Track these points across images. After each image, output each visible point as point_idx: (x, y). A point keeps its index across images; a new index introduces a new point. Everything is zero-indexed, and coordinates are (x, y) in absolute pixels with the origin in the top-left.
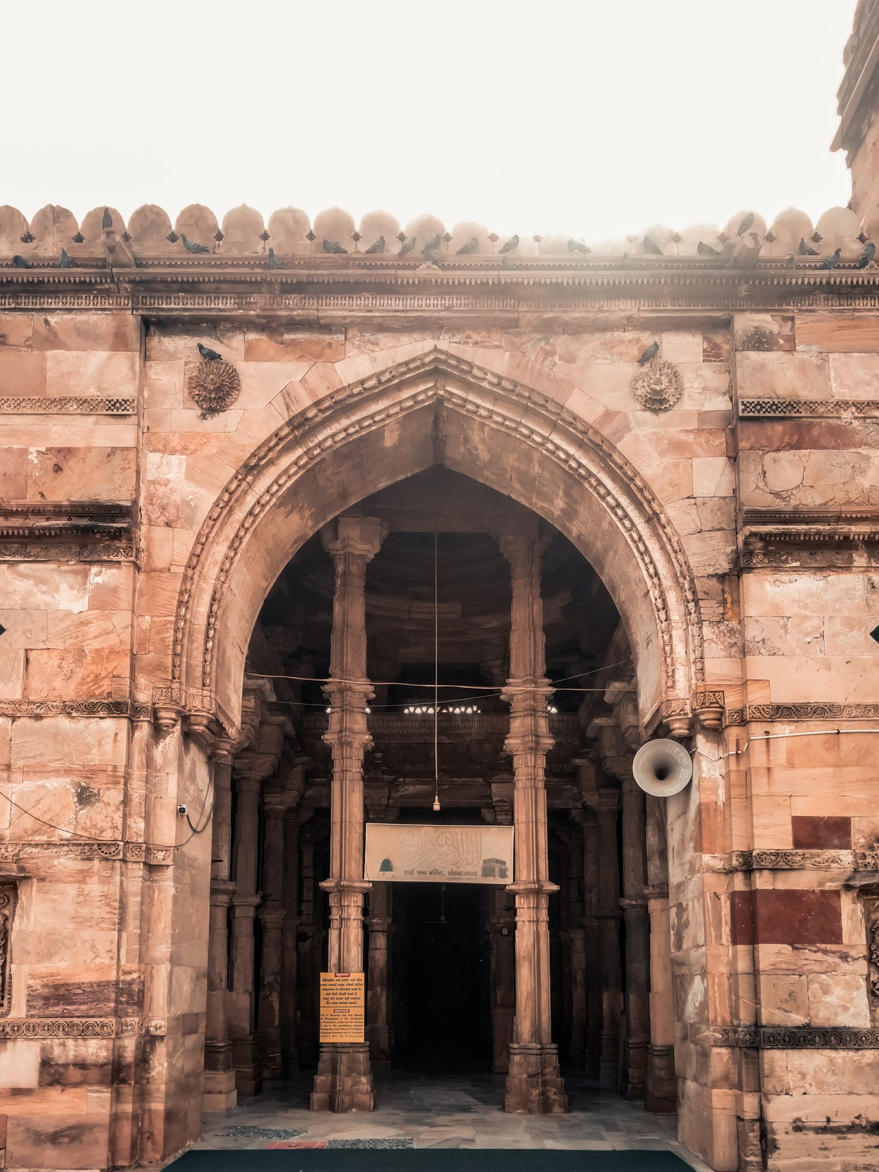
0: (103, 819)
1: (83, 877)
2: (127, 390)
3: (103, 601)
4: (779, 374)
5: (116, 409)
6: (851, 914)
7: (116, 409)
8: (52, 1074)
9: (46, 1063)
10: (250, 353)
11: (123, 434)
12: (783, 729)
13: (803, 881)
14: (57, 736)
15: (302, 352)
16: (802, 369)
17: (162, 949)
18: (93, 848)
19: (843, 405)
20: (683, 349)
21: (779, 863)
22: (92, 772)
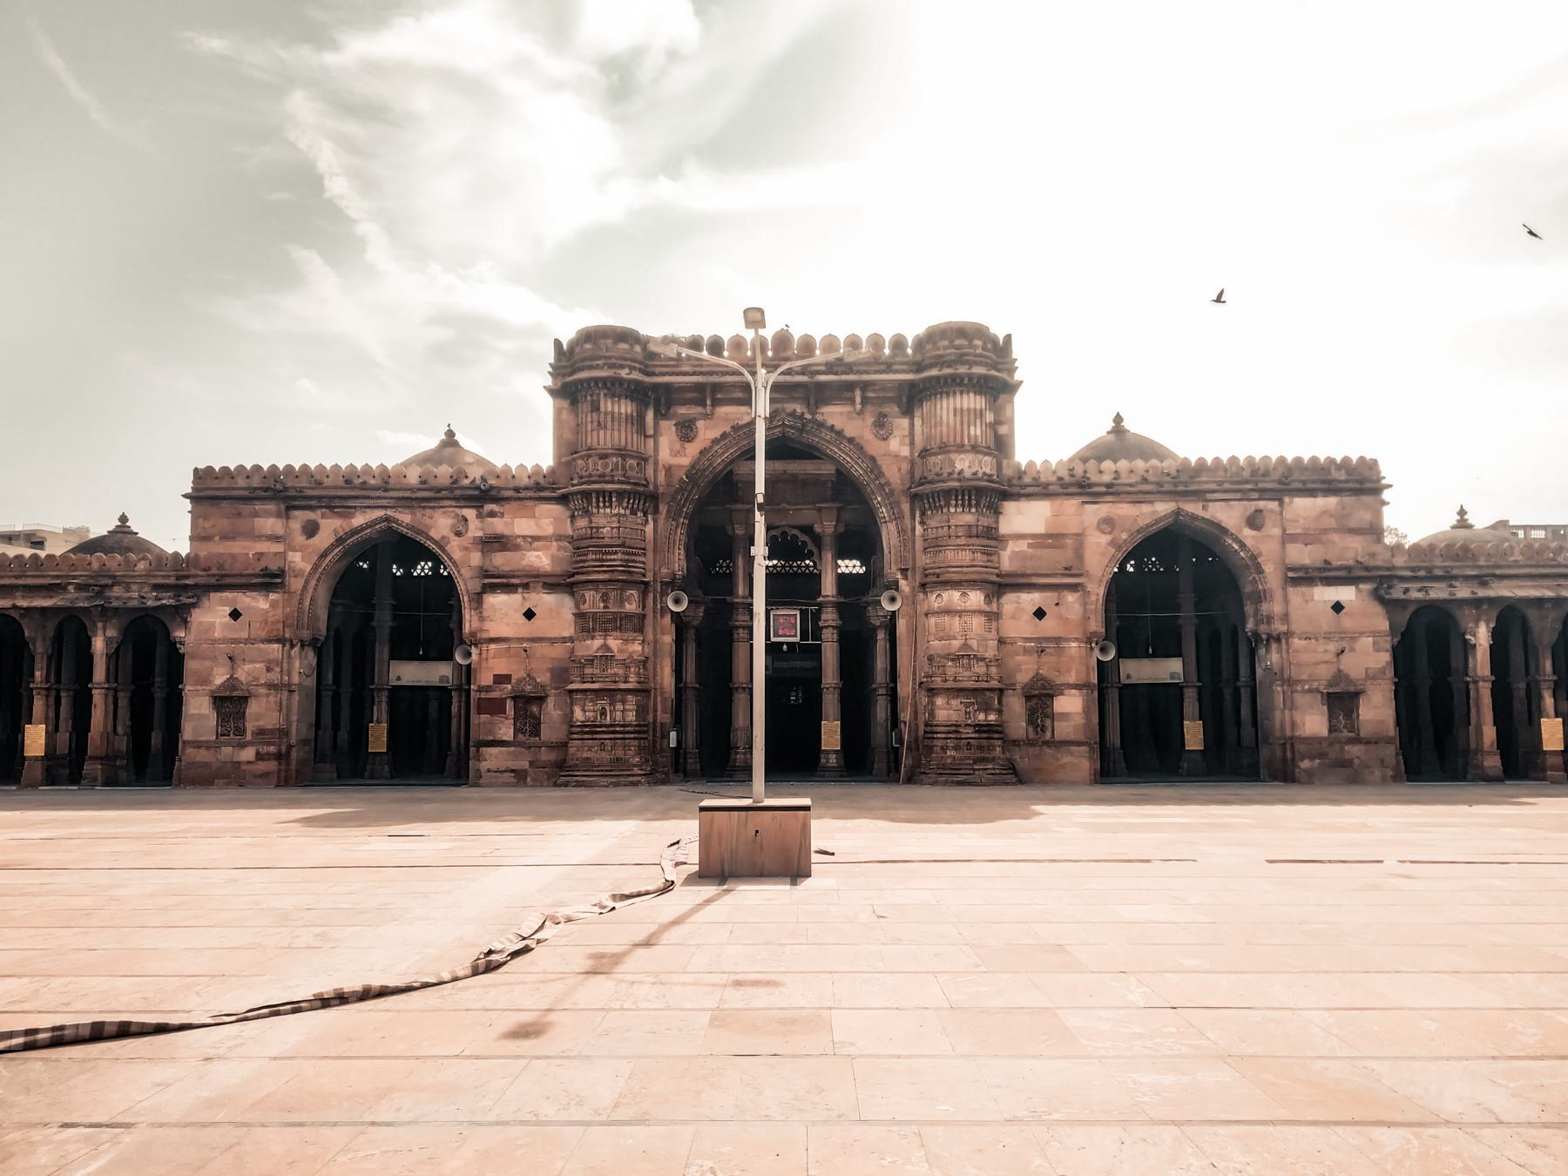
0: (275, 676)
1: (268, 695)
2: (281, 532)
3: (274, 605)
4: (498, 525)
5: (276, 538)
6: (509, 704)
7: (276, 538)
8: (260, 757)
9: (258, 753)
10: (323, 516)
11: (279, 548)
12: (493, 646)
14: (259, 650)
16: (506, 524)
17: (295, 718)
18: (271, 686)
20: (470, 513)
21: (488, 689)
22: (270, 662)
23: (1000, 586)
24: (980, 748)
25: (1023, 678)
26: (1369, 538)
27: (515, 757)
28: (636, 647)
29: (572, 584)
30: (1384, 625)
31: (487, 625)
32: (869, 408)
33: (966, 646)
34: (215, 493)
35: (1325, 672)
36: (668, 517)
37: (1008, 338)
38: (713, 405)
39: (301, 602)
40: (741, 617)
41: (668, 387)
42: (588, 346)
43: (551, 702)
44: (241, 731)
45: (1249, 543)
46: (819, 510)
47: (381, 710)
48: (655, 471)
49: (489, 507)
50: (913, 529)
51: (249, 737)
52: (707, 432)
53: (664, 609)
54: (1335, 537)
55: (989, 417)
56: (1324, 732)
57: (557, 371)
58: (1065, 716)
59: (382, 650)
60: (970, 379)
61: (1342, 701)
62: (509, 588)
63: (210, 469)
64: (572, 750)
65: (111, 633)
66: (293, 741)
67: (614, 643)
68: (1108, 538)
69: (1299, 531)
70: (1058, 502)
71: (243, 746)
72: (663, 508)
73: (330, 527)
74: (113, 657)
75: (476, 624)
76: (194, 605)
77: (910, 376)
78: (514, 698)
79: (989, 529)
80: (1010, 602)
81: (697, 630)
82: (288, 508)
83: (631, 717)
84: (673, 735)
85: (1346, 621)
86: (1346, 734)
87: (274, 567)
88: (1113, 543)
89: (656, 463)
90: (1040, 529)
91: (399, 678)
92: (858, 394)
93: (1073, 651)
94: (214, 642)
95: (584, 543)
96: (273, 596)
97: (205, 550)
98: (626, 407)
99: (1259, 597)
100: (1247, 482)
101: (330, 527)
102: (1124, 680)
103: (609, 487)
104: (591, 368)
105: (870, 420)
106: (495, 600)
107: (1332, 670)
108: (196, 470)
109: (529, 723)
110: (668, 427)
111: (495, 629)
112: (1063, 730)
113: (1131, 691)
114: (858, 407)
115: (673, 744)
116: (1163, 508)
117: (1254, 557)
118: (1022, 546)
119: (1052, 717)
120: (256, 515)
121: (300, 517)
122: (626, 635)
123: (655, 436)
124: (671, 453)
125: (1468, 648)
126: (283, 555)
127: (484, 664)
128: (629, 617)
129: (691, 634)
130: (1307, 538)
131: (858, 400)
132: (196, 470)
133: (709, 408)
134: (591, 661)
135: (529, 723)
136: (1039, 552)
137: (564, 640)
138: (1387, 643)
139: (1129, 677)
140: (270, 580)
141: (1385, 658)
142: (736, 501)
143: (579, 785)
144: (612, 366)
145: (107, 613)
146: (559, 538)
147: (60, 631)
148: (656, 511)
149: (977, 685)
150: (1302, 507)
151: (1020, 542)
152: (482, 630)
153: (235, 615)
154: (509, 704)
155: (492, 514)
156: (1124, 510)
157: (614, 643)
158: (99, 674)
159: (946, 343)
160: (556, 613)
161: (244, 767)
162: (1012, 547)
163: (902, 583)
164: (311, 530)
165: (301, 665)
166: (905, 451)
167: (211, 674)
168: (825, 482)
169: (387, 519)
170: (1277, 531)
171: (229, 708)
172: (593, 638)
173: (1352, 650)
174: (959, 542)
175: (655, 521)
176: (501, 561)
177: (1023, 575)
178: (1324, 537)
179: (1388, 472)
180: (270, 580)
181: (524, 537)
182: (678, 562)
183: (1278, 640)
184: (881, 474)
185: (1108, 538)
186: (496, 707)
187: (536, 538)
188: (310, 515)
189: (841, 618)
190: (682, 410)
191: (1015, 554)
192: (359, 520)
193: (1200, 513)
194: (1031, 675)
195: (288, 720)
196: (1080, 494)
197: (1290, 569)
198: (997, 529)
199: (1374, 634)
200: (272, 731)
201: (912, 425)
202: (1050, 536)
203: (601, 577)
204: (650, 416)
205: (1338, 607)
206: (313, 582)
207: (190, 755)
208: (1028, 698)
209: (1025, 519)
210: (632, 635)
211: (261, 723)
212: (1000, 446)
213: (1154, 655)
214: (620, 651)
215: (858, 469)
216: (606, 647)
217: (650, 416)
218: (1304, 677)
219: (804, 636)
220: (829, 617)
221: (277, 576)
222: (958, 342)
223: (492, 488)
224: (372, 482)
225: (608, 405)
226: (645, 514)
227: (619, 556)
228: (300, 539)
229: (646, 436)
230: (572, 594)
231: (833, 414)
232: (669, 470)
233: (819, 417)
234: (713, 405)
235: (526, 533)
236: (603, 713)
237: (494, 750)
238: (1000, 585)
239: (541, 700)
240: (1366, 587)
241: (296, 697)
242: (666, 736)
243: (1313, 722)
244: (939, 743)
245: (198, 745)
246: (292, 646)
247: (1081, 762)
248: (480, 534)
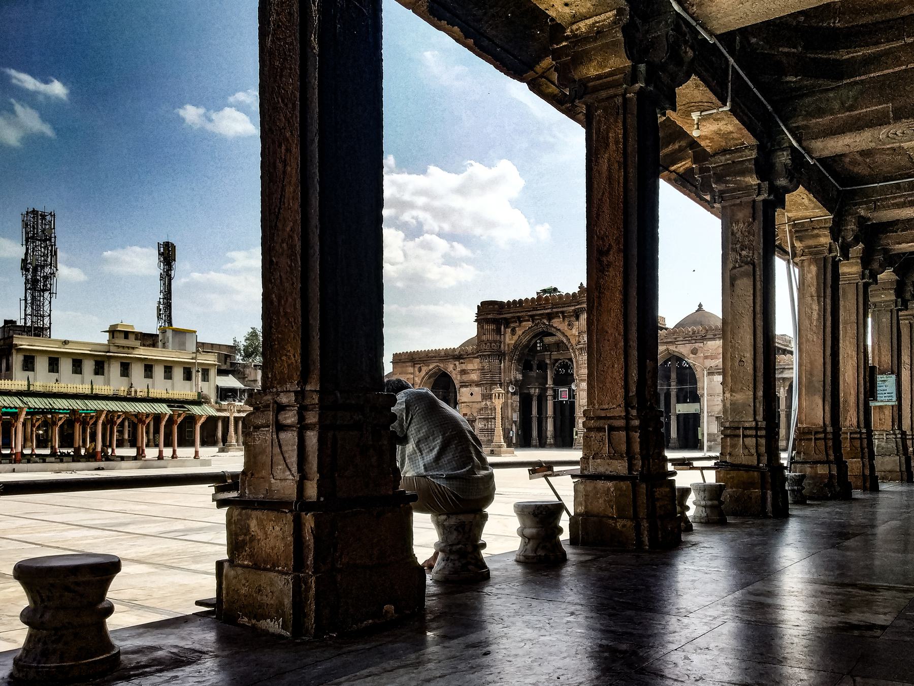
4: (464, 367)
20: (457, 363)
38: (520, 322)
41: (505, 319)
52: (519, 332)
62: (466, 386)
73: (425, 369)
98: (492, 327)
106: (463, 390)
110: (509, 330)
134: (481, 409)
148: (505, 359)
164: (420, 370)
192: (431, 367)
219: (570, 398)
231: (556, 322)
232: (508, 345)
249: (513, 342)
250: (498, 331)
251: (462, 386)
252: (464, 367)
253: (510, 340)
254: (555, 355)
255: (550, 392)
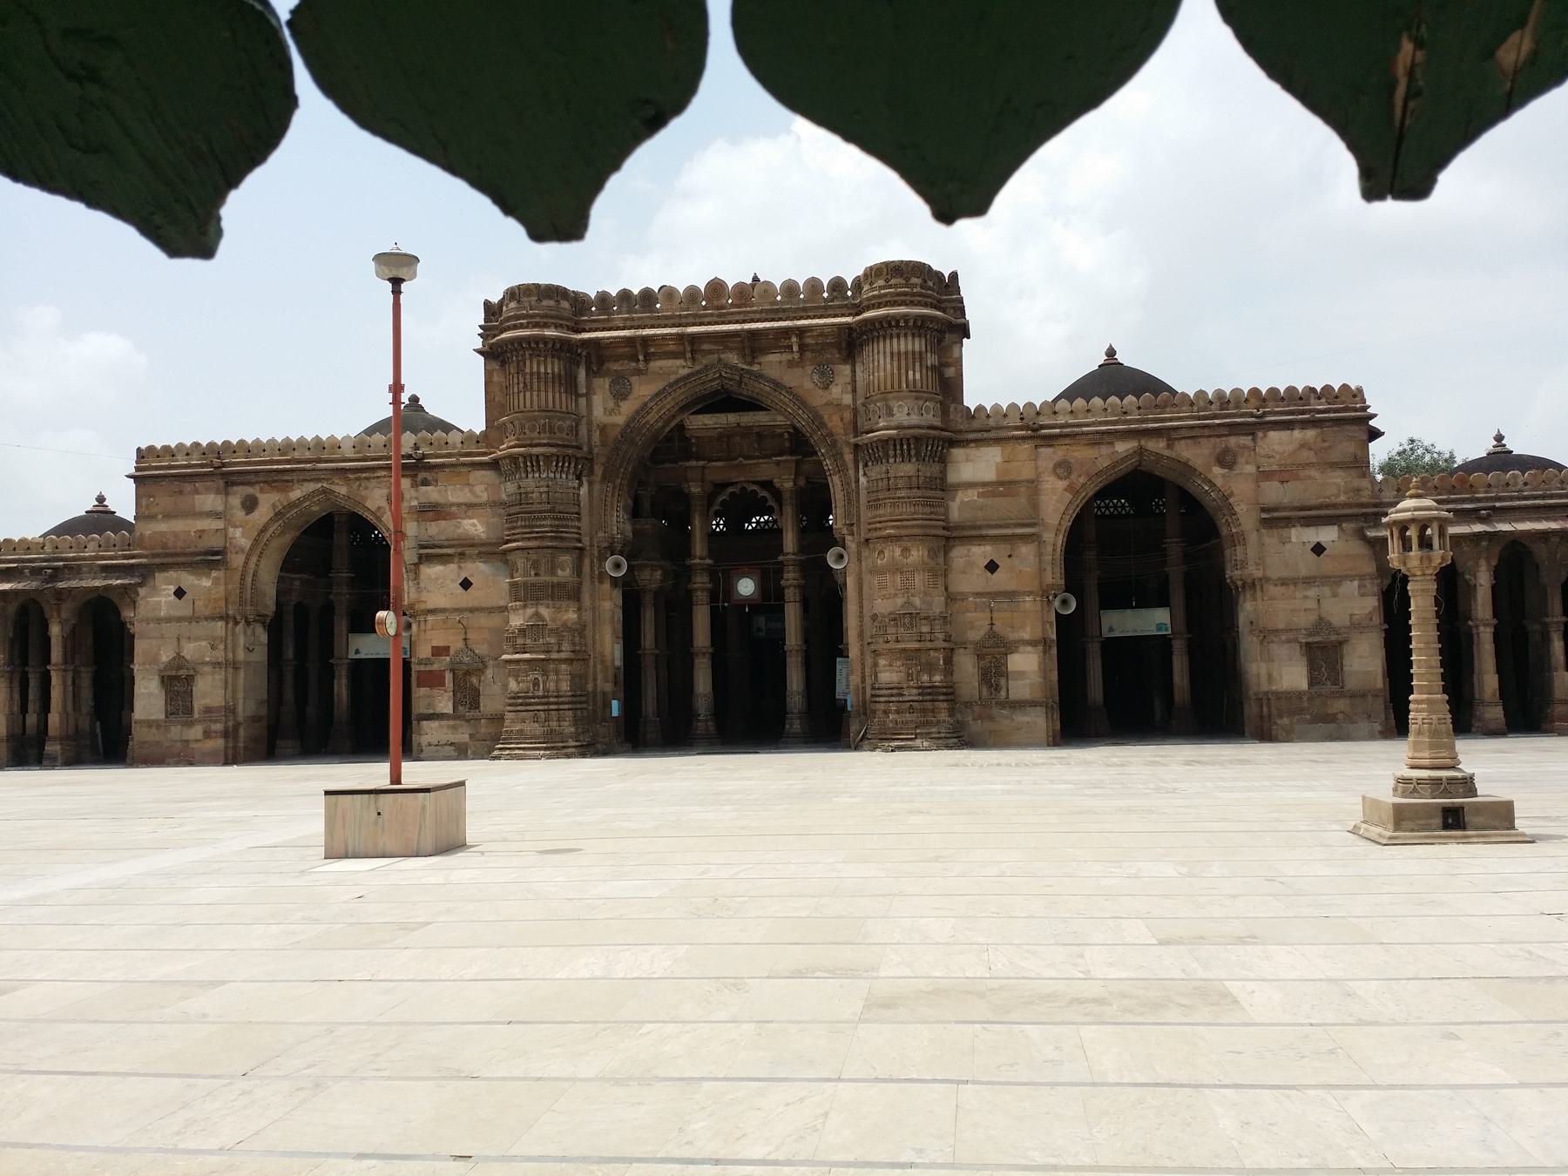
0: (219, 655)
2: (220, 508)
3: (216, 581)
4: (432, 494)
8: (207, 734)
10: (262, 491)
11: (220, 524)
13: (435, 667)
15: (279, 490)
17: (241, 695)
18: (216, 664)
19: (452, 505)
20: (406, 483)
21: (427, 662)
22: (214, 639)
23: (947, 537)
24: (924, 711)
25: (975, 635)
26: (1353, 472)
27: (454, 727)
28: (571, 616)
29: (505, 552)
30: (1371, 568)
31: (425, 596)
32: (809, 355)
33: (908, 603)
34: (158, 473)
35: (1305, 620)
36: (604, 478)
37: (954, 276)
38: (646, 361)
39: (243, 578)
40: (698, 579)
42: (513, 305)
43: (489, 673)
44: (189, 710)
45: (1219, 482)
46: (778, 463)
47: (341, 688)
48: (589, 431)
49: (422, 475)
50: (857, 481)
51: (196, 715)
52: (643, 390)
53: (603, 575)
54: (1313, 473)
55: (931, 360)
56: (1303, 684)
57: (487, 332)
58: (1021, 674)
59: (341, 624)
60: (906, 322)
61: (1323, 654)
62: (444, 559)
63: (151, 449)
64: (507, 723)
65: (64, 615)
66: (241, 719)
67: (545, 612)
68: (1065, 483)
69: (1275, 467)
70: (1009, 447)
71: (190, 724)
72: (599, 470)
73: (268, 502)
74: (71, 640)
75: (413, 596)
76: (141, 585)
77: (849, 319)
78: (453, 671)
79: (932, 479)
80: (959, 554)
81: (657, 594)
82: (227, 484)
83: (565, 686)
84: (615, 704)
85: (1326, 564)
86: (1329, 687)
87: (216, 543)
88: (1069, 489)
89: (590, 423)
90: (989, 475)
91: (357, 652)
92: (794, 339)
93: (1028, 605)
94: (159, 620)
95: (513, 510)
96: (214, 574)
97: (149, 529)
98: (553, 367)
99: (1239, 539)
100: (1215, 417)
101: (268, 502)
102: (1106, 634)
103: (535, 450)
104: (515, 327)
105: (809, 369)
106: (431, 571)
107: (1313, 618)
108: (139, 450)
109: (468, 697)
111: (435, 599)
112: (1020, 689)
113: (1118, 649)
114: (796, 356)
115: (615, 713)
116: (1122, 447)
117: (1226, 498)
118: (971, 495)
119: (1006, 675)
120: (197, 492)
121: (242, 491)
122: (558, 604)
123: (588, 395)
124: (606, 410)
125: (1471, 589)
126: (225, 529)
127: (422, 636)
128: (561, 585)
129: (648, 599)
130: (1284, 474)
131: (795, 348)
132: (139, 450)
133: (641, 365)
135: (468, 697)
136: (989, 501)
137: (504, 609)
138: (1373, 587)
139: (1111, 630)
140: (210, 559)
141: (1371, 603)
142: (688, 460)
143: (512, 757)
144: (536, 325)
145: (60, 595)
146: (494, 504)
147: (23, 611)
148: (591, 472)
149: (917, 645)
150: (1278, 443)
151: (970, 492)
152: (420, 602)
153: (180, 593)
154: (448, 677)
155: (425, 483)
156: (1081, 454)
157: (545, 612)
158: (56, 654)
159: (881, 282)
160: (491, 583)
161: (192, 745)
162: (963, 497)
163: (848, 538)
164: (250, 505)
165: (251, 644)
166: (847, 399)
167: (158, 655)
168: (781, 435)
169: (324, 491)
170: (1251, 469)
171: (178, 687)
172: (525, 607)
173: (1335, 595)
174: (899, 494)
175: (590, 483)
176: (436, 530)
177: (974, 527)
178: (1302, 474)
179: (1374, 403)
180: (210, 559)
181: (459, 505)
182: (618, 524)
183: (1253, 585)
184: (822, 425)
185: (1065, 483)
186: (434, 680)
187: (470, 506)
188: (249, 490)
189: (804, 577)
190: (615, 367)
191: (962, 502)
192: (296, 494)
193: (1167, 453)
194: (982, 633)
195: (234, 698)
196: (1031, 438)
197: (1263, 510)
198: (943, 478)
199: (1362, 577)
200: (218, 709)
201: (854, 372)
202: (1001, 483)
203: (530, 544)
204: (582, 374)
205: (1318, 549)
206: (254, 559)
207: (139, 734)
208: (980, 657)
209: (976, 466)
210: (564, 604)
211: (208, 701)
212: (948, 386)
213: (1137, 607)
214: (553, 620)
215: (802, 421)
216: (537, 614)
217: (582, 374)
218: (1281, 626)
220: (790, 577)
221: (216, 553)
222: (893, 282)
223: (424, 456)
224: (308, 455)
225: (532, 366)
226: (579, 477)
227: (549, 522)
228: (239, 514)
229: (578, 395)
230: (506, 562)
231: (772, 363)
232: (603, 429)
233: (755, 368)
234: (646, 361)
235: (461, 500)
236: (536, 683)
237: (435, 724)
238: (947, 538)
239: (481, 671)
240: (1349, 526)
241: (242, 674)
242: (608, 706)
243: (1292, 675)
244: (882, 707)
245: (149, 724)
246: (236, 623)
247: (1038, 720)
248: (415, 503)
249: (620, 420)
250: (568, 384)
251: (425, 559)
252: (432, 494)
253: (610, 412)
254: (718, 470)
255: (701, 581)
